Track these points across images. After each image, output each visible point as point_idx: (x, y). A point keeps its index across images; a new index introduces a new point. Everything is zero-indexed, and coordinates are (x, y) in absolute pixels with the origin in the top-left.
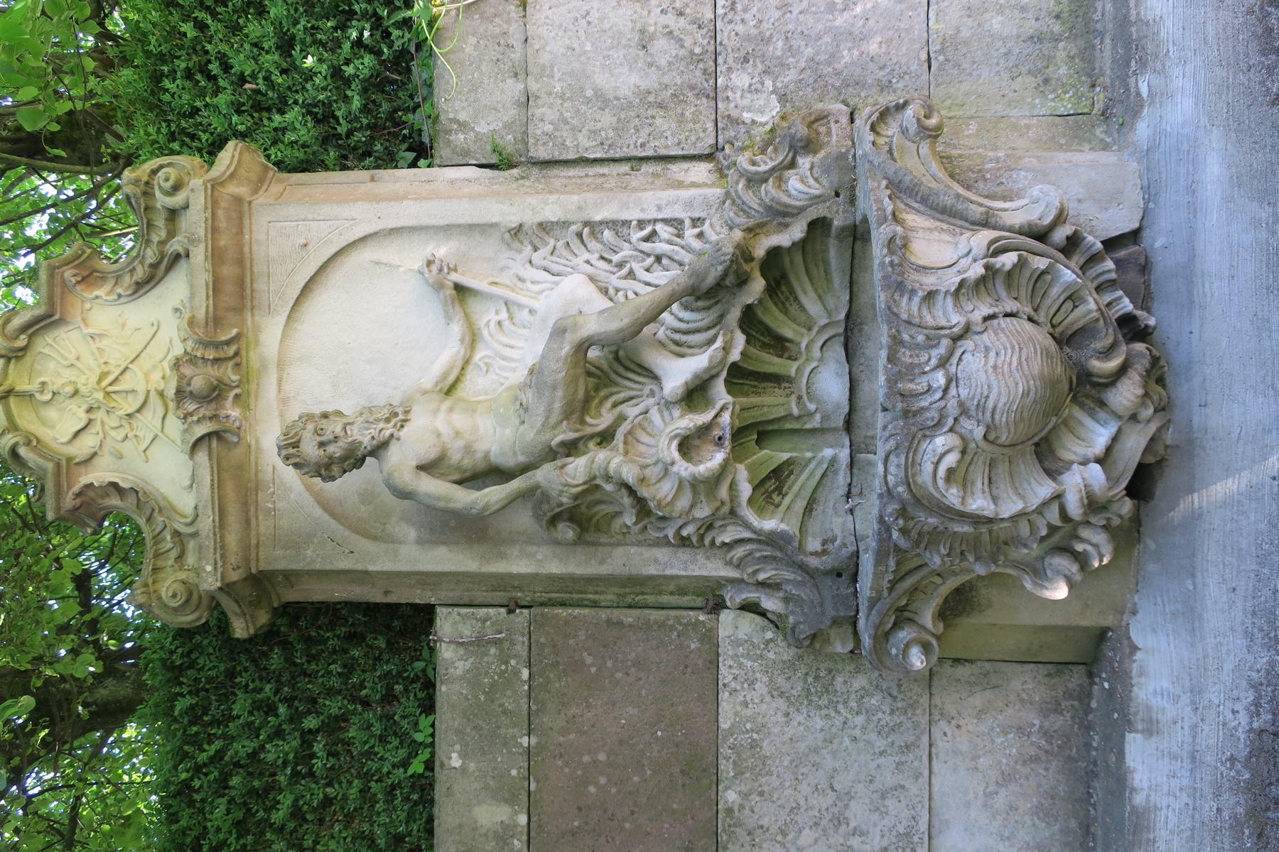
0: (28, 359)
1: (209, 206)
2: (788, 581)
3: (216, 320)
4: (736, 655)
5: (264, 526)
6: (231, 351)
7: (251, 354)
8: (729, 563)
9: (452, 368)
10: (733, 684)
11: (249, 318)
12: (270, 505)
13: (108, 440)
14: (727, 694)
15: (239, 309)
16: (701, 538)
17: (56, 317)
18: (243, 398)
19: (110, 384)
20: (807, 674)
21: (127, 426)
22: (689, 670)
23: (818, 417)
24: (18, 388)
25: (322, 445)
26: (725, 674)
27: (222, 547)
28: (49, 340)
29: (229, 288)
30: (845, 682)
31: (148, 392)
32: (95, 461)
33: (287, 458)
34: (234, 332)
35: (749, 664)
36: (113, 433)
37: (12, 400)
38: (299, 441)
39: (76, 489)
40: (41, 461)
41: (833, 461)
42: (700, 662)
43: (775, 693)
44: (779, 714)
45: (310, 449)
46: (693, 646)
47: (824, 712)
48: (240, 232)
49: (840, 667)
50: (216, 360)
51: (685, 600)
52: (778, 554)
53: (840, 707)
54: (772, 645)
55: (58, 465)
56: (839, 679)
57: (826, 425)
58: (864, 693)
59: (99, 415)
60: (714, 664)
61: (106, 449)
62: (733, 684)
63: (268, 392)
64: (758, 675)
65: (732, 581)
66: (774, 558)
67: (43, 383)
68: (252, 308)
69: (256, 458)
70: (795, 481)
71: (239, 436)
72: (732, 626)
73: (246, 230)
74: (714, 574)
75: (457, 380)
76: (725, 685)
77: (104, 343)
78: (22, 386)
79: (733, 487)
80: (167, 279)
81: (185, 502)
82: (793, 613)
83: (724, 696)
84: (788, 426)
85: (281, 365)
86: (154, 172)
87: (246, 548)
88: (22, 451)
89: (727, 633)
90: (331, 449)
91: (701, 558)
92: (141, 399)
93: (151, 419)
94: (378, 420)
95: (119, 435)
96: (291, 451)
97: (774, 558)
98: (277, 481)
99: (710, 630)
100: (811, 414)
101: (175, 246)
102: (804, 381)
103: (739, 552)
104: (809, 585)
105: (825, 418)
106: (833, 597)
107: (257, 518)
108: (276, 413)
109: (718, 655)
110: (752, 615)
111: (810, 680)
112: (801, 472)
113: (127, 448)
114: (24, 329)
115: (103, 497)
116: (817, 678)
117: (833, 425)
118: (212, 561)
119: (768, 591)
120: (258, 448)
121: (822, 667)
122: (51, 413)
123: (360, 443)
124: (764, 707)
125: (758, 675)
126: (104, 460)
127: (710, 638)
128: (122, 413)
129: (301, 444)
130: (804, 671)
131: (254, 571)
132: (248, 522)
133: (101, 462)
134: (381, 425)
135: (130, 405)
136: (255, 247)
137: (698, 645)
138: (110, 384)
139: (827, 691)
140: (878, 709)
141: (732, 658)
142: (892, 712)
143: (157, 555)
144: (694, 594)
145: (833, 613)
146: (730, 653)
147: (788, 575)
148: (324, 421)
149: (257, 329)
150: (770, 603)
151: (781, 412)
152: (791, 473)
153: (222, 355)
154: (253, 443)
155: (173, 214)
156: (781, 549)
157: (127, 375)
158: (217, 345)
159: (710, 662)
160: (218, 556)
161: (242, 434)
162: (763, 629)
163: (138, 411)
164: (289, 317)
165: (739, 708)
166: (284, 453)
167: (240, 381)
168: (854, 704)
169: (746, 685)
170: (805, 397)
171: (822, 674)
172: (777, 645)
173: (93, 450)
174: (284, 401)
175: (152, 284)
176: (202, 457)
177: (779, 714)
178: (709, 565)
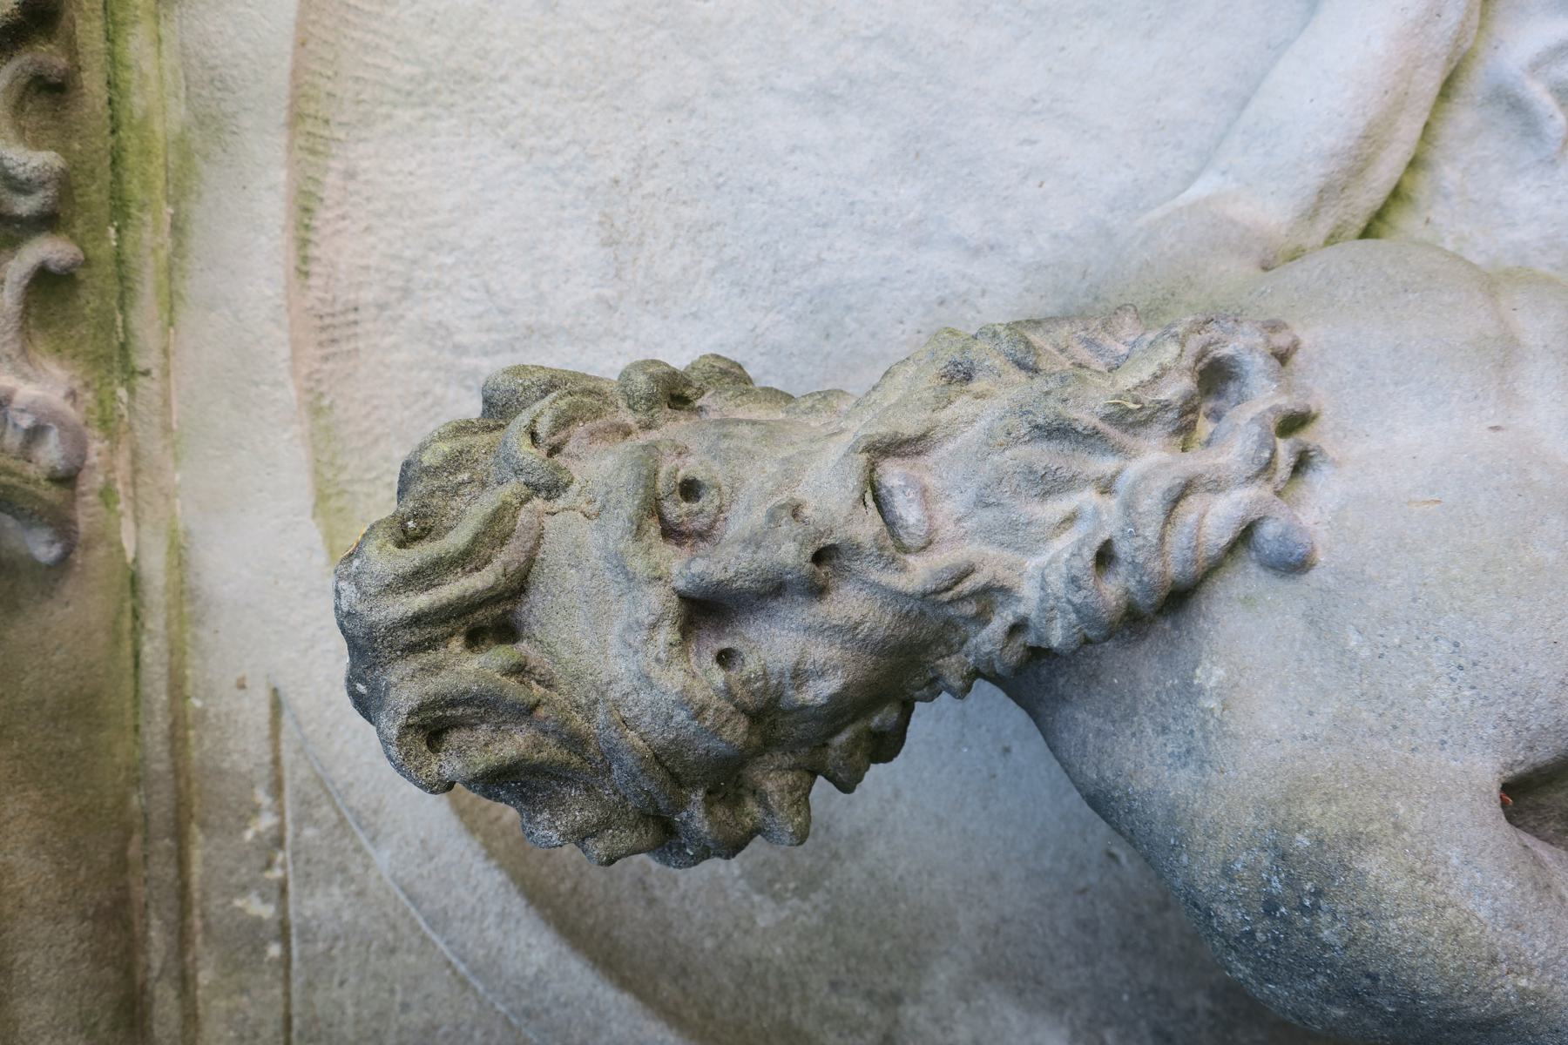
7: (137, 44)
9: (1398, 104)
12: (267, 911)
18: (89, 301)
25: (705, 610)
33: (432, 727)
38: (518, 587)
45: (612, 651)
69: (176, 652)
71: (62, 526)
75: (1397, 195)
85: (308, 120)
90: (776, 645)
94: (1130, 419)
96: (470, 668)
98: (296, 775)
107: (185, 982)
108: (290, 393)
120: (184, 593)
123: (991, 595)
129: (536, 609)
134: (1152, 460)
148: (674, 427)
154: (155, 566)
161: (86, 516)
166: (407, 686)
167: (65, 184)
174: (330, 330)
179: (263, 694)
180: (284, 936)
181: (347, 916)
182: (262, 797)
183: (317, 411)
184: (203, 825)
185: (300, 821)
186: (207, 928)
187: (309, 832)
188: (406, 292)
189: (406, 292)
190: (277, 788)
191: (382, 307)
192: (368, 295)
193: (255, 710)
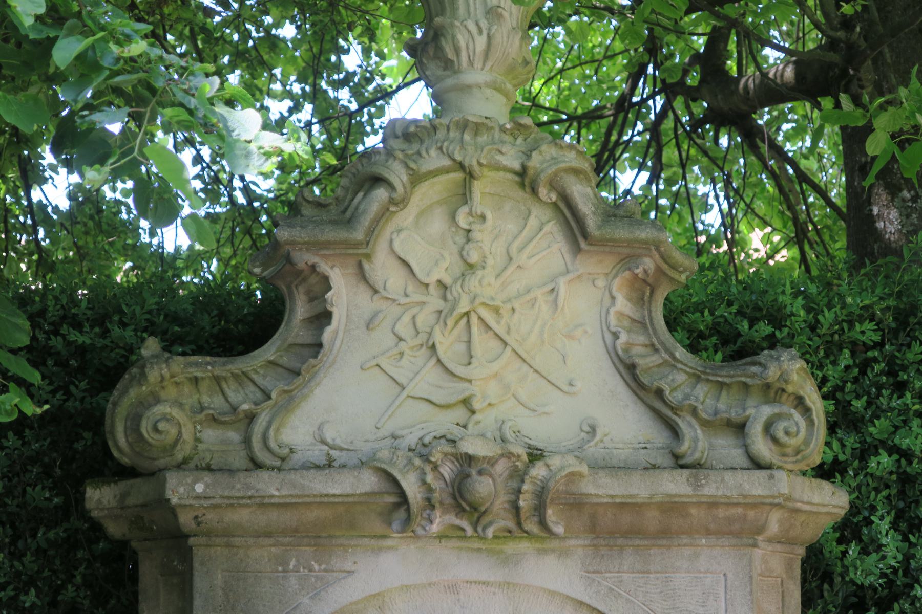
0: (520, 194)
1: (747, 501)
3: (576, 504)
5: (261, 555)
6: (531, 526)
11: (580, 542)
12: (291, 567)
13: (395, 310)
15: (593, 528)
17: (583, 244)
19: (480, 318)
21: (418, 341)
24: (476, 183)
27: (232, 504)
28: (548, 227)
29: (626, 519)
31: (470, 381)
32: (362, 287)
34: (559, 529)
36: (406, 318)
37: (458, 176)
39: (324, 267)
40: (366, 221)
48: (708, 532)
50: (516, 509)
55: (357, 245)
59: (434, 301)
61: (383, 305)
63: (465, 566)
67: (483, 218)
68: (594, 546)
73: (713, 539)
77: (544, 307)
78: (478, 187)
80: (641, 408)
81: (297, 432)
85: (506, 586)
86: (799, 402)
87: (228, 533)
88: (381, 194)
92: (460, 371)
93: (428, 380)
95: (403, 328)
101: (688, 427)
113: (383, 337)
114: (566, 199)
115: (308, 292)
118: (210, 493)
120: (380, 549)
122: (437, 224)
126: (365, 302)
128: (438, 337)
131: (192, 541)
132: (268, 534)
133: (363, 296)
135: (448, 344)
136: (687, 551)
138: (480, 318)
143: (217, 380)
149: (564, 553)
153: (523, 516)
154: (389, 542)
155: (739, 428)
157: (495, 344)
158: (540, 509)
160: (218, 501)
163: (439, 361)
164: (581, 603)
173: (379, 286)
175: (633, 385)
176: (368, 482)
179: (353, 569)
180: (284, 571)
181: (290, 589)
182: (323, 567)
183: (430, 584)
184: (316, 550)
185: (317, 577)
186: (287, 550)
187: (313, 579)
188: (463, 607)
189: (463, 607)
190: (326, 571)
191: (459, 600)
192: (462, 597)
193: (348, 566)
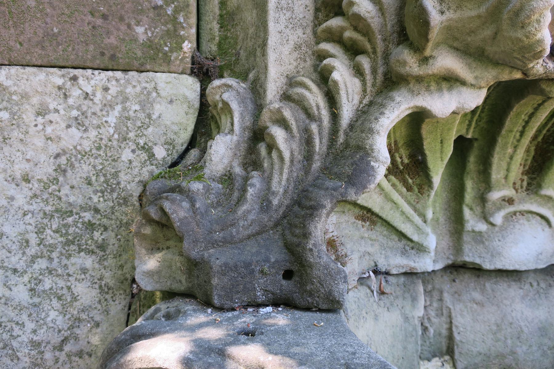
2: (268, 181)
4: (126, 99)
8: (292, 82)
10: (76, 92)
14: (60, 82)
16: (335, 37)
20: (97, 211)
22: (99, 22)
23: (482, 227)
26: (92, 81)
30: (84, 271)
35: (112, 119)
41: (419, 248)
42: (112, 40)
43: (63, 160)
44: (27, 166)
46: (140, 30)
47: (33, 239)
49: (111, 261)
51: (213, 26)
52: (316, 165)
53: (42, 264)
54: (144, 156)
56: (89, 262)
57: (466, 238)
58: (66, 299)
60: (110, 64)
62: (76, 92)
64: (93, 133)
65: (257, 90)
66: (308, 157)
70: (401, 194)
72: (173, 97)
74: (272, 56)
76: (74, 79)
79: (450, 80)
82: (208, 189)
83: (57, 77)
84: (469, 185)
89: (161, 85)
91: (299, 35)
97: (308, 157)
99: (167, 60)
100: (485, 218)
102: (534, 208)
103: (315, 98)
104: (265, 218)
105: (478, 237)
106: (247, 265)
109: (125, 71)
110: (191, 127)
111: (87, 216)
112: (409, 203)
116: (90, 226)
117: (466, 248)
119: (244, 146)
121: (110, 235)
124: (39, 142)
125: (93, 133)
127: (151, 59)
130: (101, 206)
137: (142, 38)
139: (68, 243)
140: (40, 323)
141: (121, 92)
142: (35, 345)
144: (224, 39)
145: (216, 264)
146: (129, 90)
147: (281, 183)
150: (222, 151)
151: (496, 174)
152: (409, 189)
156: (326, 170)
159: (113, 57)
162: (170, 143)
165: (35, 100)
168: (47, 283)
169: (75, 113)
170: (511, 209)
171: (96, 235)
172: (143, 164)
177: (27, 166)
178: (287, 49)
